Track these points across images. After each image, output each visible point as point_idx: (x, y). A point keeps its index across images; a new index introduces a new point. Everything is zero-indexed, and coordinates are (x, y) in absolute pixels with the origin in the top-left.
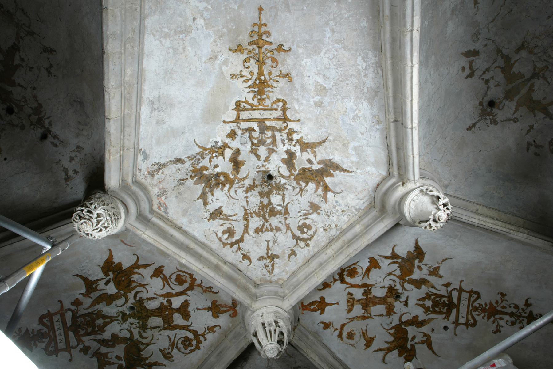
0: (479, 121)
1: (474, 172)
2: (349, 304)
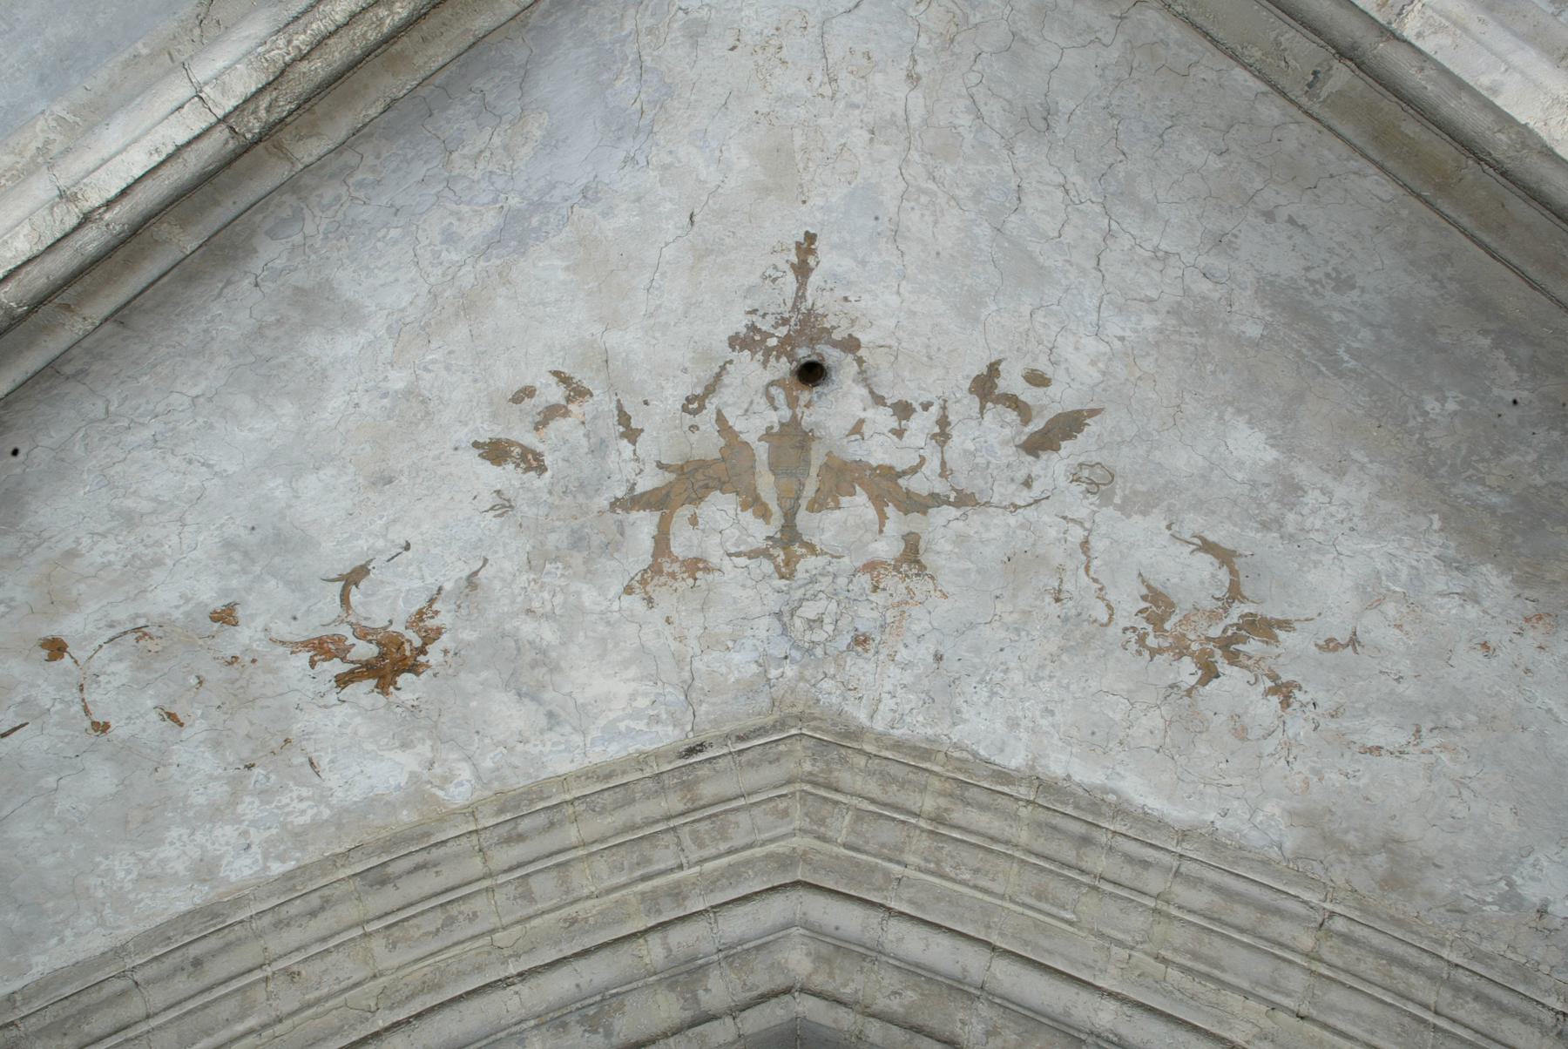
0: (800, 296)
1: (638, 130)
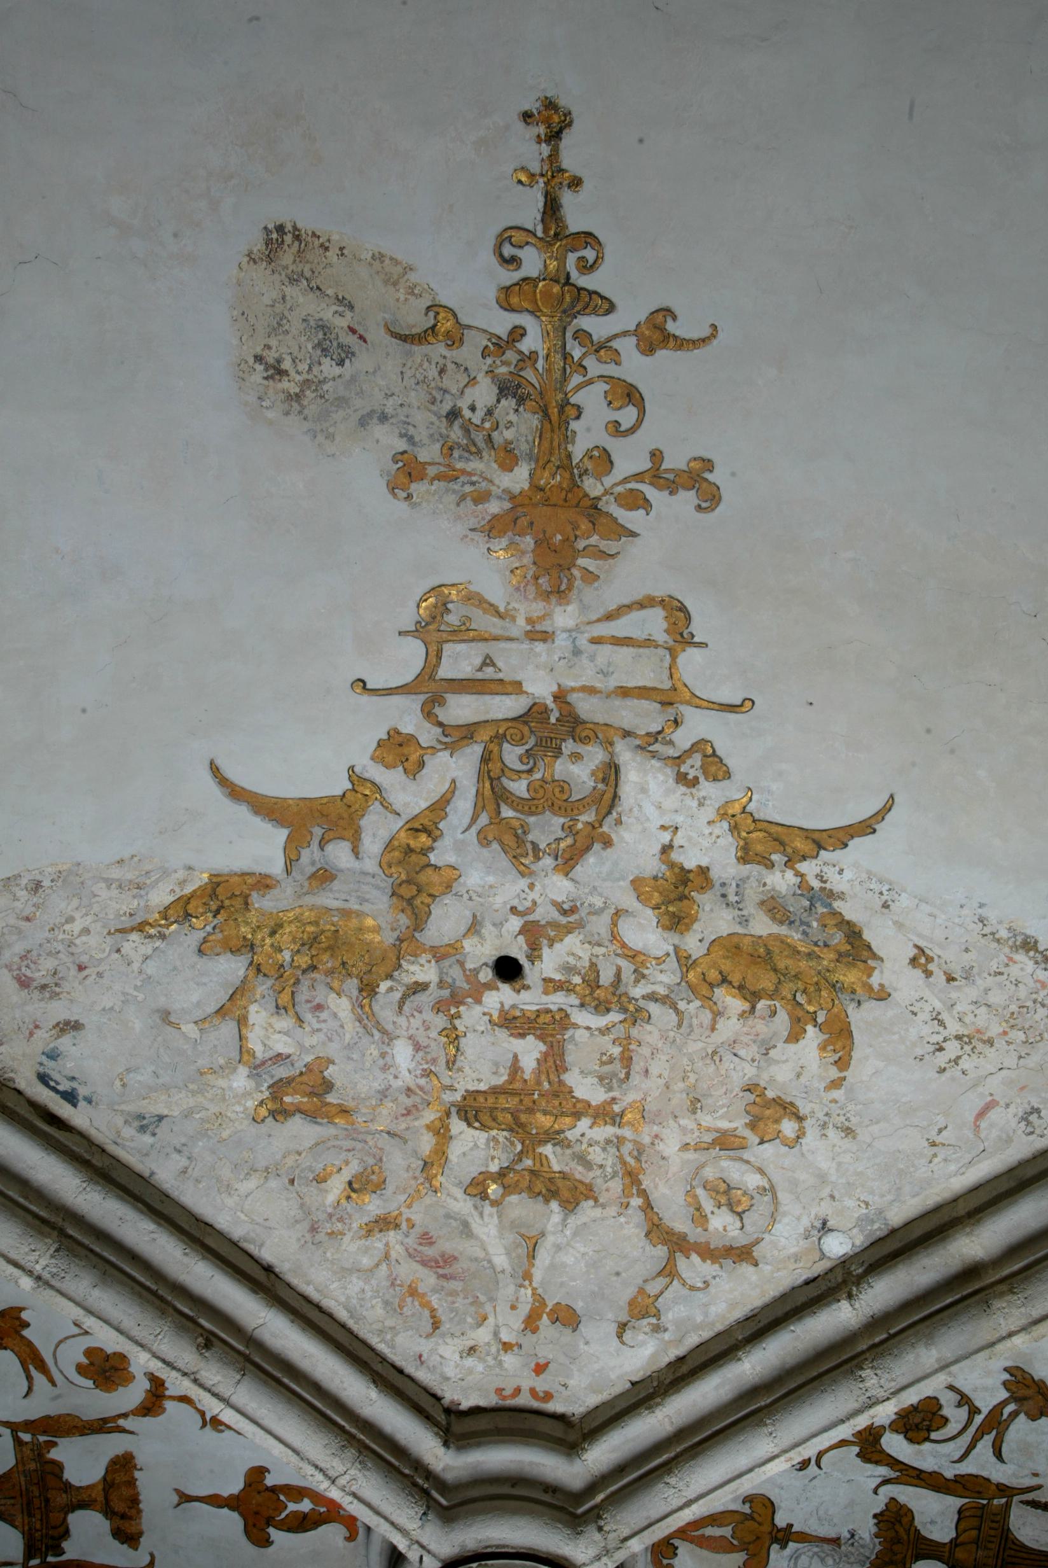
2: (126, 1492)
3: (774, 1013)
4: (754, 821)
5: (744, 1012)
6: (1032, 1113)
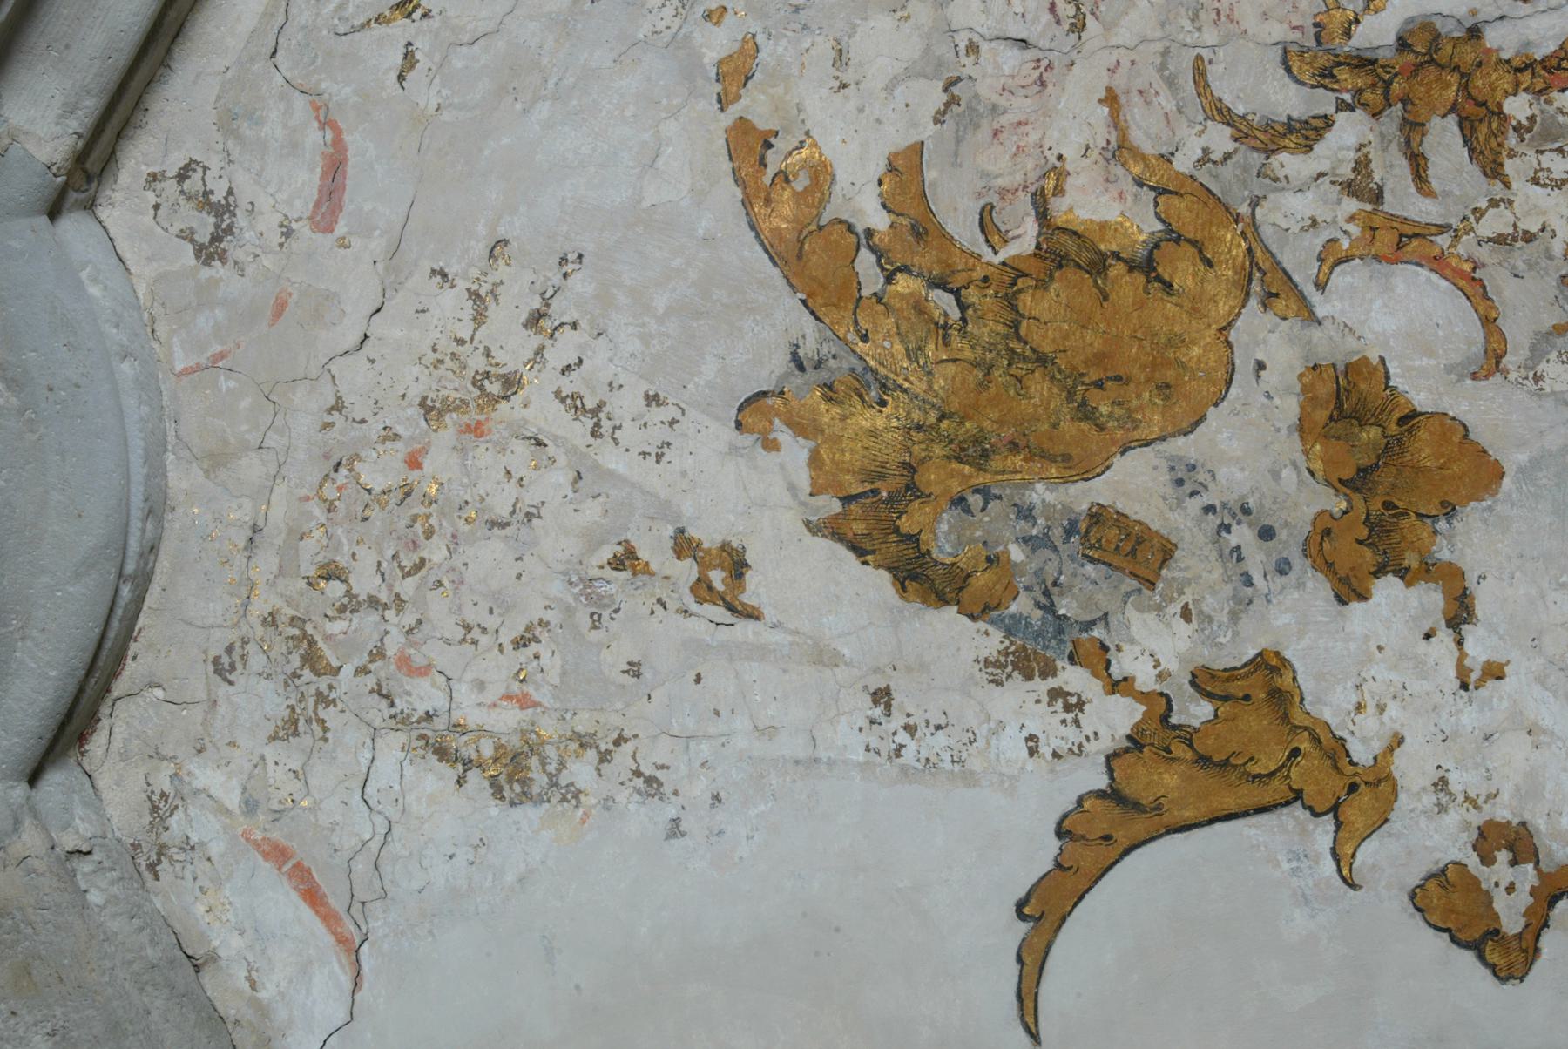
3: (986, 222)
4: (1298, 795)
5: (1059, 191)
6: (216, 238)
